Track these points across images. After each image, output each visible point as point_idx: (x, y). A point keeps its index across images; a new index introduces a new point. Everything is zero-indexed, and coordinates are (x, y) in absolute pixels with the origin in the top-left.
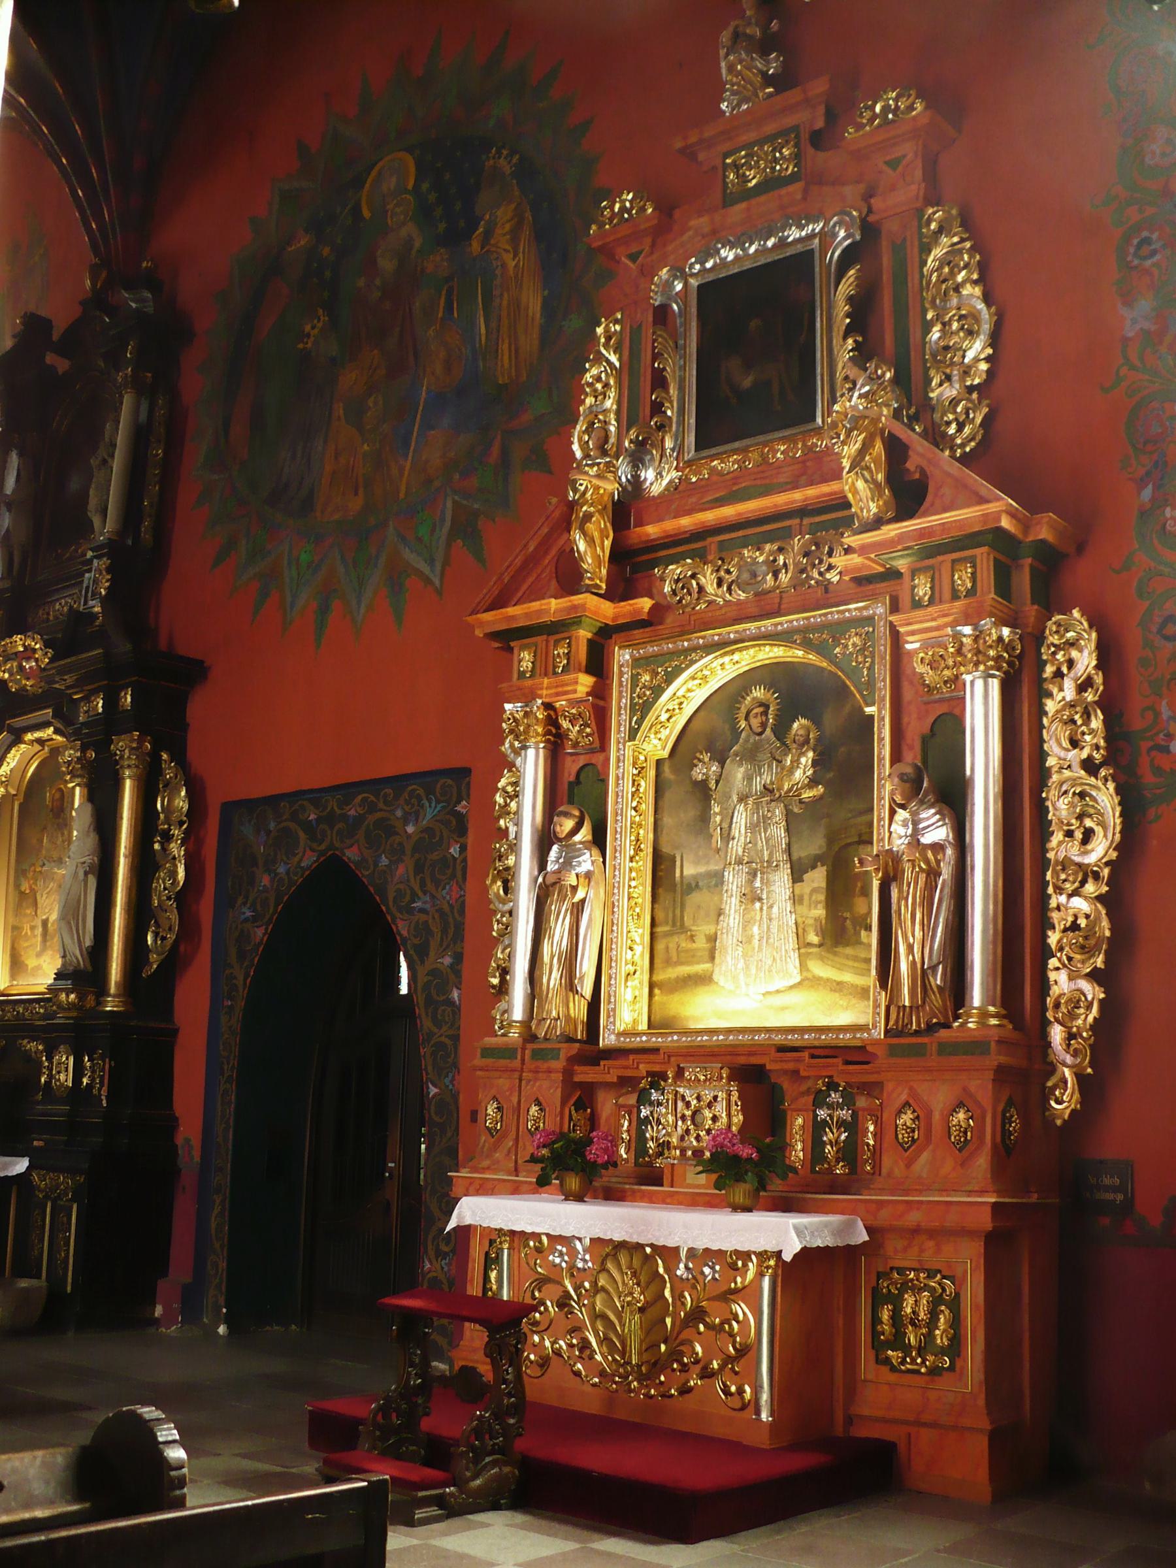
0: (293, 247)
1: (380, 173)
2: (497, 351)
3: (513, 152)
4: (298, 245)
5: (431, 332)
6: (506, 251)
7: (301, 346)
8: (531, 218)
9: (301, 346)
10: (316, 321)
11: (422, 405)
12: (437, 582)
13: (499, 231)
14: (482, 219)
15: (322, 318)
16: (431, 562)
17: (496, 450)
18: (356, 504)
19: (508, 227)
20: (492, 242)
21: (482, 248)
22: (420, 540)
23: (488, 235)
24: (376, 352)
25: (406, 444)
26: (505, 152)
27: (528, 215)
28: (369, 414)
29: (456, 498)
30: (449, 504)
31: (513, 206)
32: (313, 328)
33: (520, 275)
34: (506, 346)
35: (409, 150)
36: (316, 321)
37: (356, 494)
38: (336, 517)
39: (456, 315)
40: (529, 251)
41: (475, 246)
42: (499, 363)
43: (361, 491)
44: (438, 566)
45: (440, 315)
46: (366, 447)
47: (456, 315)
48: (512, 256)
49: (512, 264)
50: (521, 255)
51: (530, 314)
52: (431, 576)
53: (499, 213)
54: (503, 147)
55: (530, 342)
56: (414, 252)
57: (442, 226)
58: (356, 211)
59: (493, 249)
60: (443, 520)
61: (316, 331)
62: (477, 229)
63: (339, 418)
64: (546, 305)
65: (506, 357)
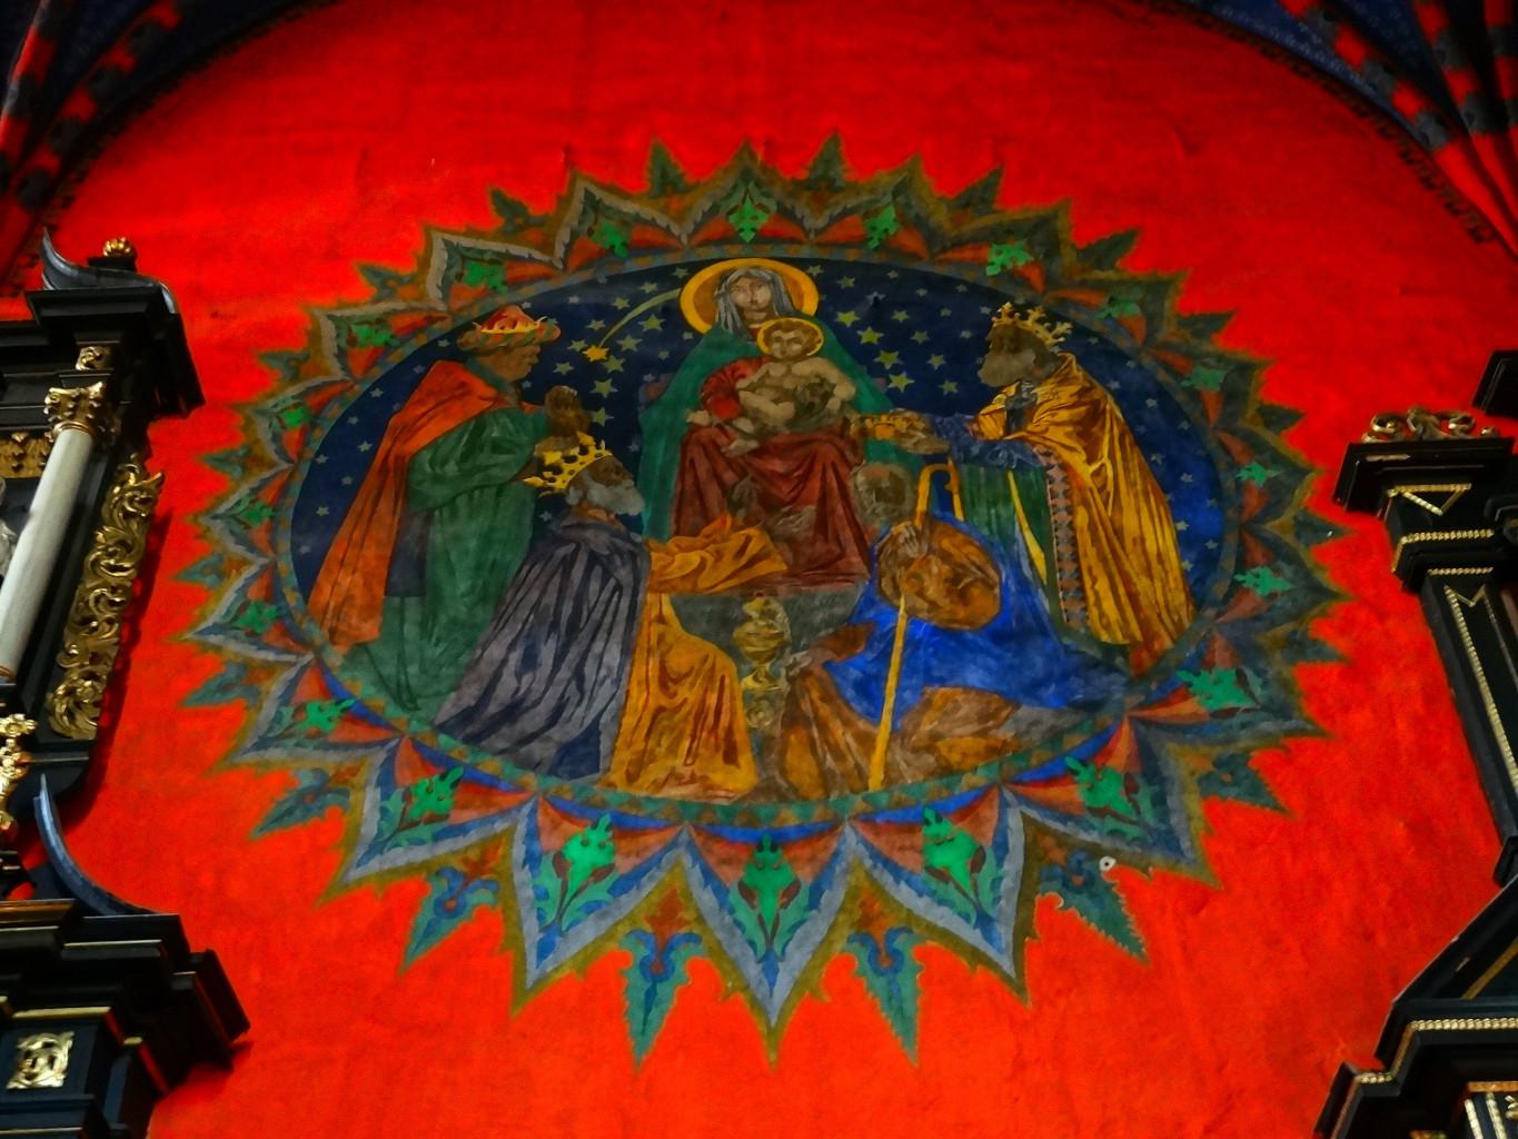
0: (496, 330)
1: (723, 277)
2: (1081, 589)
3: (1051, 318)
4: (508, 331)
5: (902, 529)
6: (1071, 449)
7: (537, 481)
8: (1119, 415)
9: (537, 481)
10: (575, 451)
11: (899, 644)
12: (1007, 964)
13: (1041, 419)
14: (998, 390)
15: (593, 451)
16: (984, 922)
17: (1123, 746)
18: (740, 778)
19: (1064, 415)
20: (1030, 427)
21: (1008, 431)
22: (942, 875)
23: (1017, 415)
24: (752, 531)
25: (869, 690)
26: (1034, 314)
27: (1110, 405)
28: (750, 627)
29: (1033, 814)
30: (1014, 821)
31: (1074, 389)
32: (571, 460)
33: (1110, 487)
34: (1103, 585)
35: (801, 264)
36: (575, 451)
37: (730, 756)
38: (675, 792)
39: (959, 515)
40: (1124, 459)
41: (990, 424)
42: (1094, 612)
43: (745, 758)
44: (1005, 933)
45: (922, 506)
46: (749, 681)
47: (959, 515)
48: (1084, 456)
49: (1085, 471)
50: (1105, 460)
51: (1151, 546)
52: (983, 946)
53: (1041, 392)
54: (1031, 305)
55: (1166, 589)
56: (834, 404)
57: (901, 382)
58: (671, 313)
59: (1034, 438)
60: (1002, 848)
61: (577, 467)
62: (989, 402)
63: (661, 619)
64: (1184, 541)
65: (1109, 605)
